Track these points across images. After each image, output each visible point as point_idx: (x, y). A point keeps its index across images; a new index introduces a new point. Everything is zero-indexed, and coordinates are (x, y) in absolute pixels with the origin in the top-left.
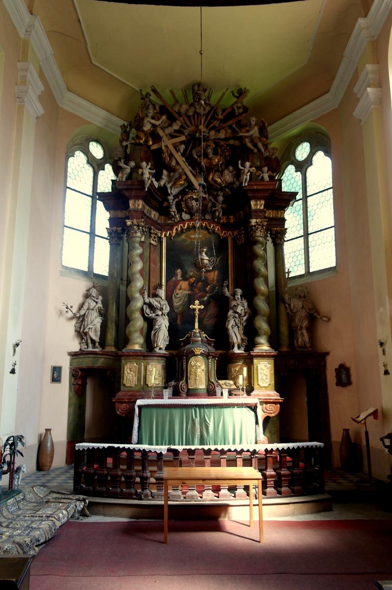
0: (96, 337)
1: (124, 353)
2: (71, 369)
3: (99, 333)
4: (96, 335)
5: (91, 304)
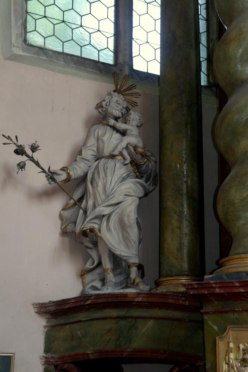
0: (127, 247)
1: (208, 286)
2: (47, 362)
3: (134, 233)
4: (126, 239)
5: (105, 138)
